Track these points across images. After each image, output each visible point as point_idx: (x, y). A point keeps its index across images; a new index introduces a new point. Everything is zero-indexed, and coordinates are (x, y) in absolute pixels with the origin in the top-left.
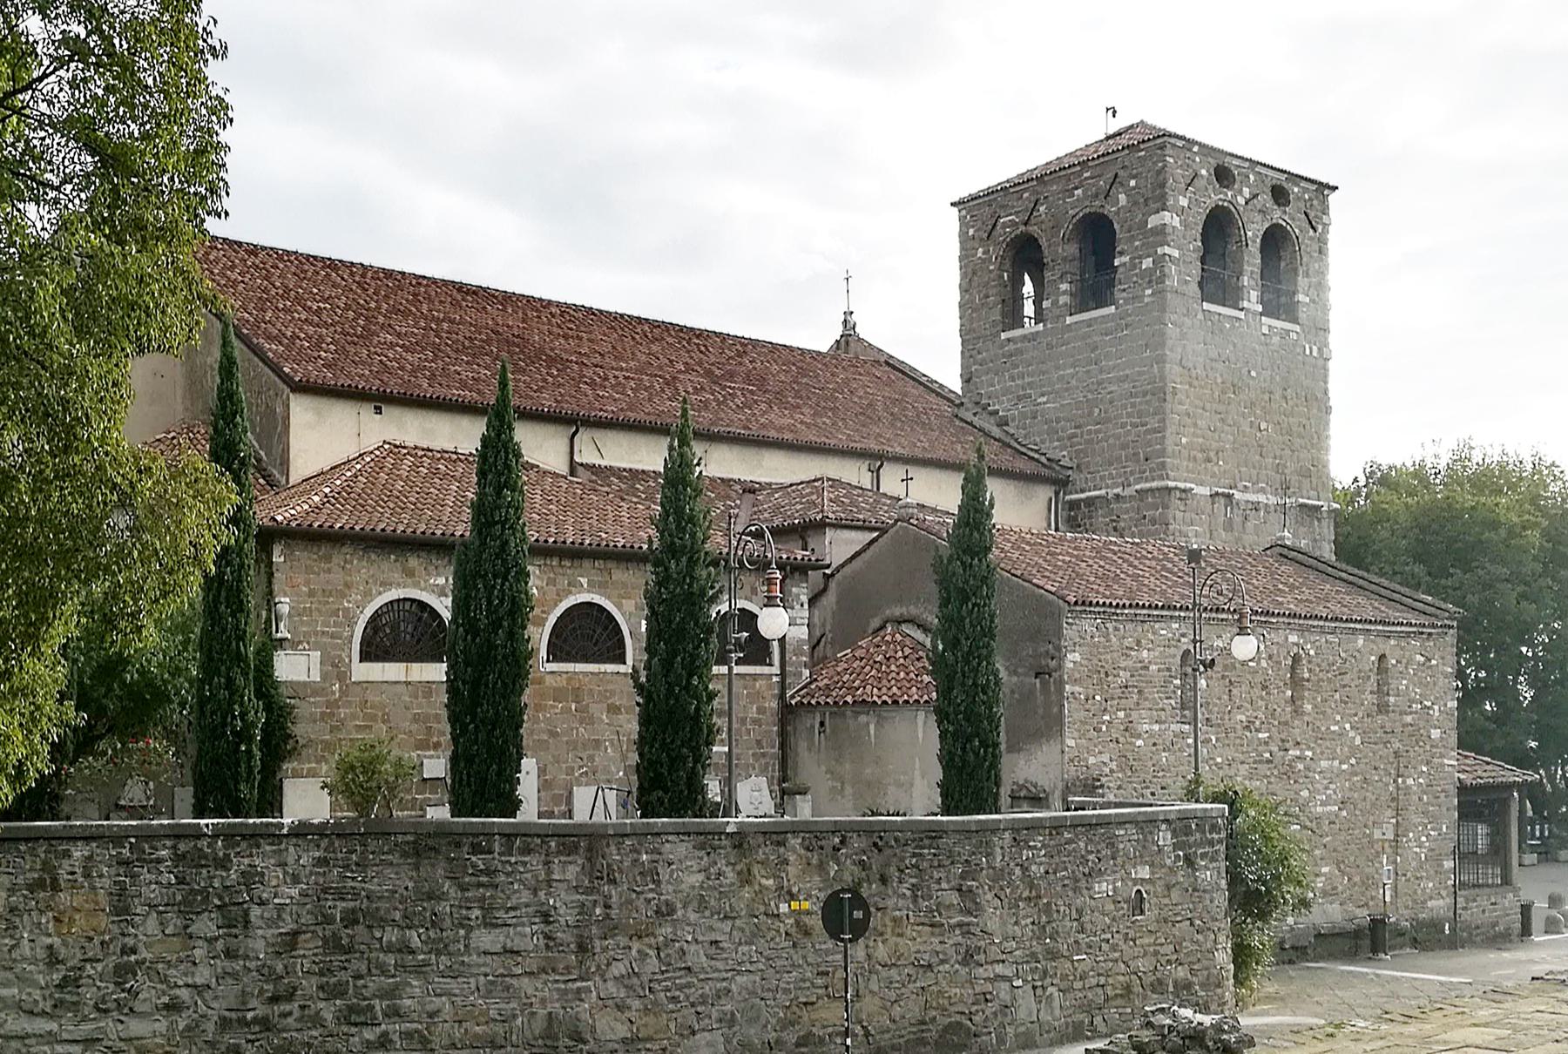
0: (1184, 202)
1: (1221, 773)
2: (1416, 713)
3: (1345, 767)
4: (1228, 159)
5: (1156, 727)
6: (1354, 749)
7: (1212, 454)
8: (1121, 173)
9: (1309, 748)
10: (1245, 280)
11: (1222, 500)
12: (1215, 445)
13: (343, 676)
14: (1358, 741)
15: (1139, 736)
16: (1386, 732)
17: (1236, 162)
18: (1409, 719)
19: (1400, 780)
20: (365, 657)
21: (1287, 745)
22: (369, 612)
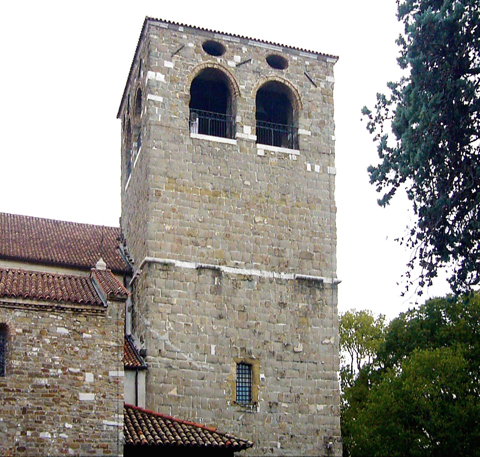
0: (169, 64)
4: (216, 36)
7: (199, 241)
10: (238, 119)
11: (210, 273)
12: (202, 232)
17: (228, 38)
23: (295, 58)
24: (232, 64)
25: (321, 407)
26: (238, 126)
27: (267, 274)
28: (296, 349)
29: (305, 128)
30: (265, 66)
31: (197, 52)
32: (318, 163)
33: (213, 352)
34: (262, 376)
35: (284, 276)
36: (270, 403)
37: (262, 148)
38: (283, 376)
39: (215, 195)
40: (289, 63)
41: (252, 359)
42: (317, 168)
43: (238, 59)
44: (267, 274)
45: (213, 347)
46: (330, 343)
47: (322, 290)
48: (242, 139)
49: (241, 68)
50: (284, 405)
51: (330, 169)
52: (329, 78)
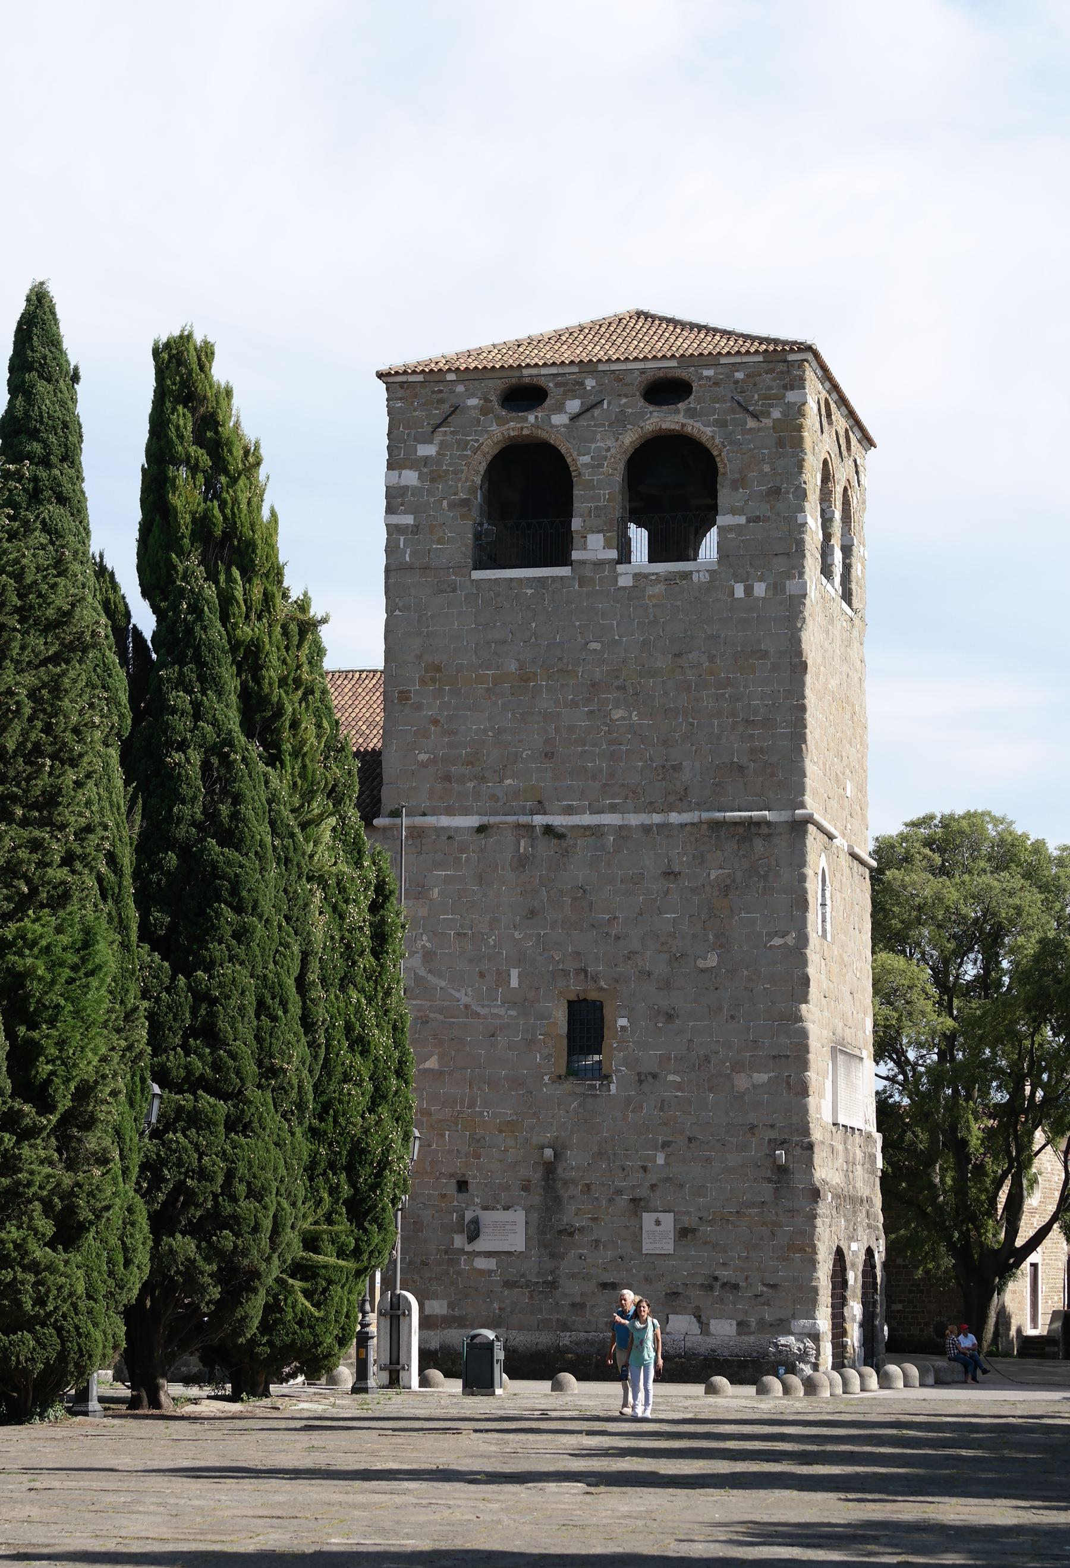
0: (427, 450)
10: (576, 524)
23: (708, 373)
24: (559, 419)
25: (762, 1078)
26: (577, 540)
31: (485, 411)
32: (761, 579)
33: (514, 983)
34: (623, 1022)
35: (675, 818)
36: (639, 1074)
38: (670, 1017)
40: (695, 385)
41: (601, 989)
42: (760, 589)
43: (574, 406)
44: (634, 820)
45: (514, 973)
47: (768, 837)
48: (583, 563)
49: (582, 422)
50: (671, 1078)
51: (791, 586)
52: (791, 396)
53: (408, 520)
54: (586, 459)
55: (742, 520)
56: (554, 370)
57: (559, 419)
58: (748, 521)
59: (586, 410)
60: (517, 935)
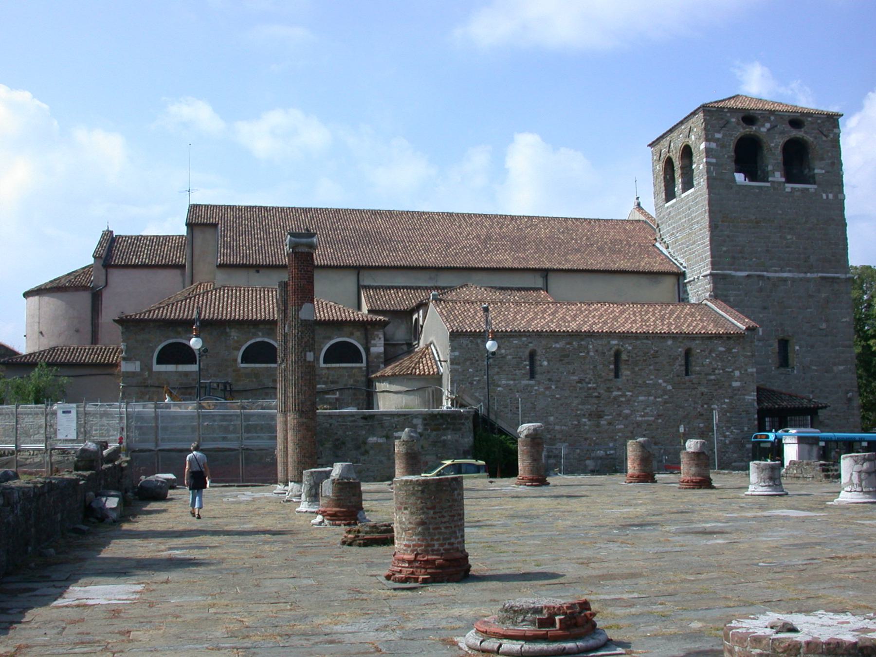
1: (560, 402)
2: (719, 374)
3: (658, 400)
5: (512, 382)
6: (665, 392)
8: (692, 126)
9: (629, 391)
10: (770, 168)
13: (150, 369)
14: (669, 387)
15: (499, 386)
16: (693, 384)
18: (713, 377)
19: (705, 406)
20: (159, 362)
21: (612, 390)
22: (160, 347)
23: (810, 119)
24: (764, 130)
25: (841, 368)
27: (797, 275)
28: (821, 327)
29: (822, 169)
30: (788, 128)
31: (738, 124)
32: (831, 193)
34: (797, 348)
37: (789, 187)
39: (757, 223)
40: (806, 124)
41: (789, 336)
43: (768, 125)
44: (797, 275)
46: (846, 321)
48: (773, 182)
49: (771, 132)
51: (840, 196)
52: (836, 131)
53: (714, 161)
54: (772, 145)
55: (823, 171)
56: (760, 112)
57: (764, 130)
58: (826, 172)
59: (773, 127)
60: (761, 316)
